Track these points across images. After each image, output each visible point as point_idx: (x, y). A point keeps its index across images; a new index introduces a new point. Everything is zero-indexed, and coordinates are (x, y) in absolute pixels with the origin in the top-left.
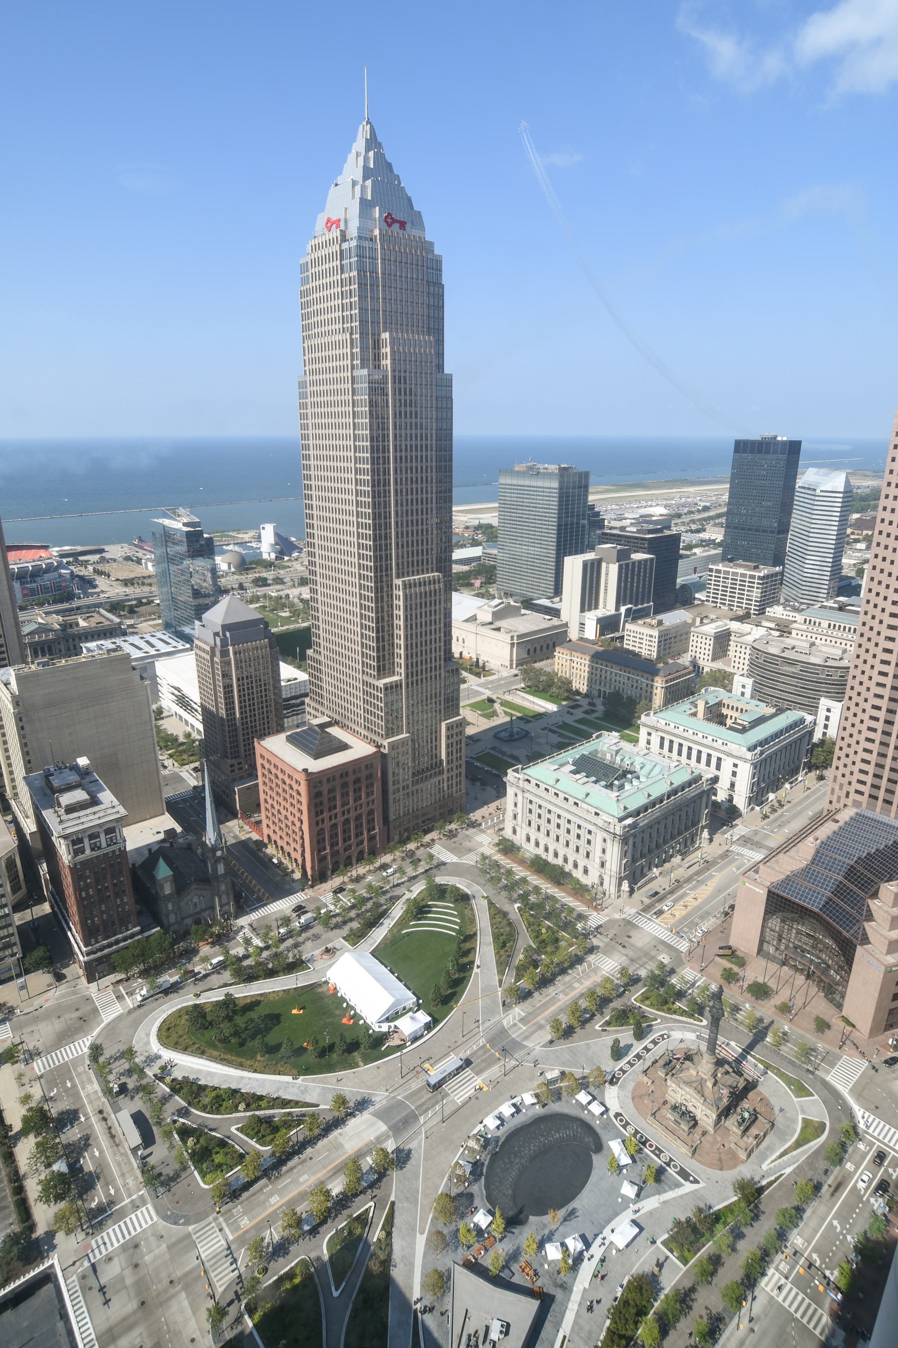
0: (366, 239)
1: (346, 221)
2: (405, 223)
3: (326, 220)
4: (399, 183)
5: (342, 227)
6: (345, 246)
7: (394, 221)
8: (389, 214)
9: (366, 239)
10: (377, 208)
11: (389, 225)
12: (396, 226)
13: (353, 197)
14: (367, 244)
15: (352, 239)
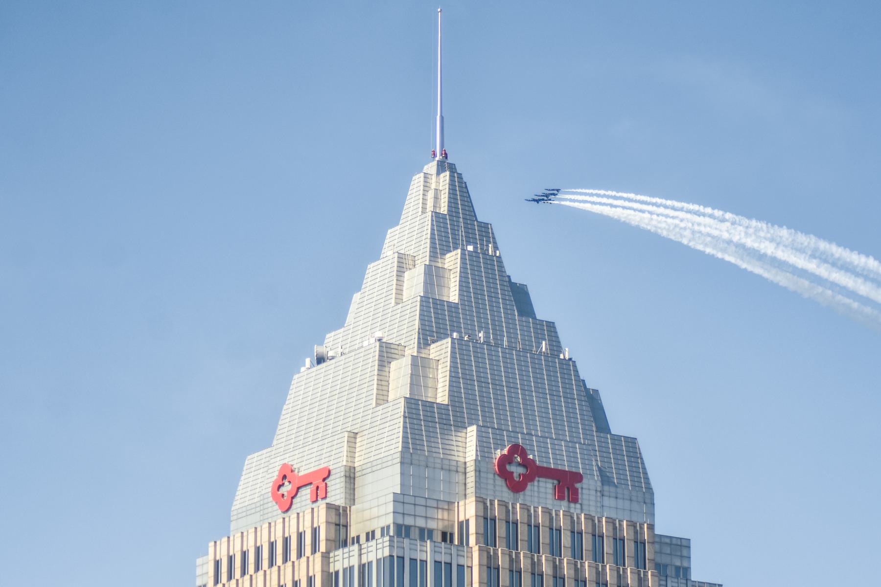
0: (425, 534)
1: (351, 476)
2: (578, 477)
3: (275, 475)
4: (556, 346)
5: (337, 494)
6: (344, 559)
7: (534, 472)
8: (516, 449)
9: (425, 534)
10: (472, 431)
11: (517, 487)
12: (544, 488)
13: (382, 397)
14: (427, 552)
15: (370, 536)
